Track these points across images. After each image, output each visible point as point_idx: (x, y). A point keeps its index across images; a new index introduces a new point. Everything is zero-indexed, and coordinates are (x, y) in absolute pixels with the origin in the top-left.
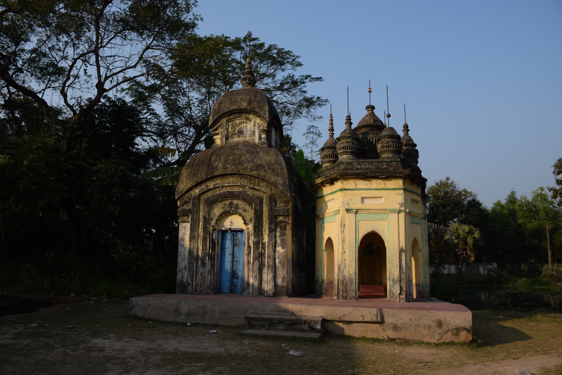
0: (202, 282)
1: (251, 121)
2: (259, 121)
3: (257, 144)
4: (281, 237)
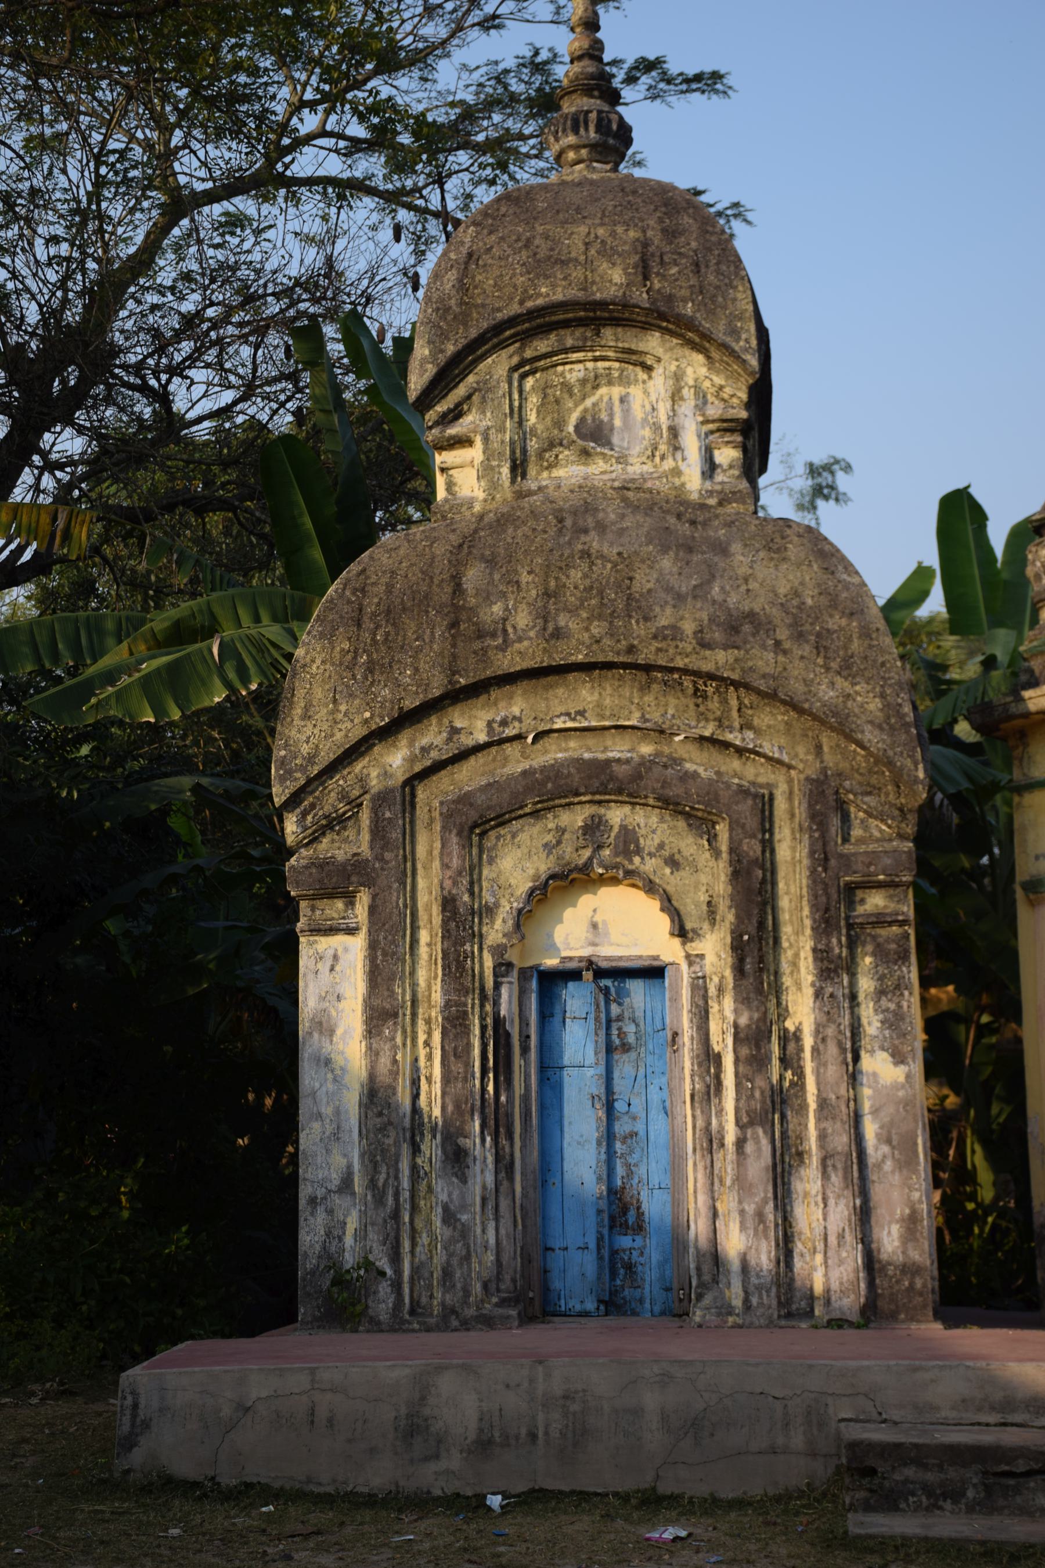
0: (455, 1261)
1: (648, 369)
2: (703, 371)
3: (694, 496)
4: (884, 1003)
